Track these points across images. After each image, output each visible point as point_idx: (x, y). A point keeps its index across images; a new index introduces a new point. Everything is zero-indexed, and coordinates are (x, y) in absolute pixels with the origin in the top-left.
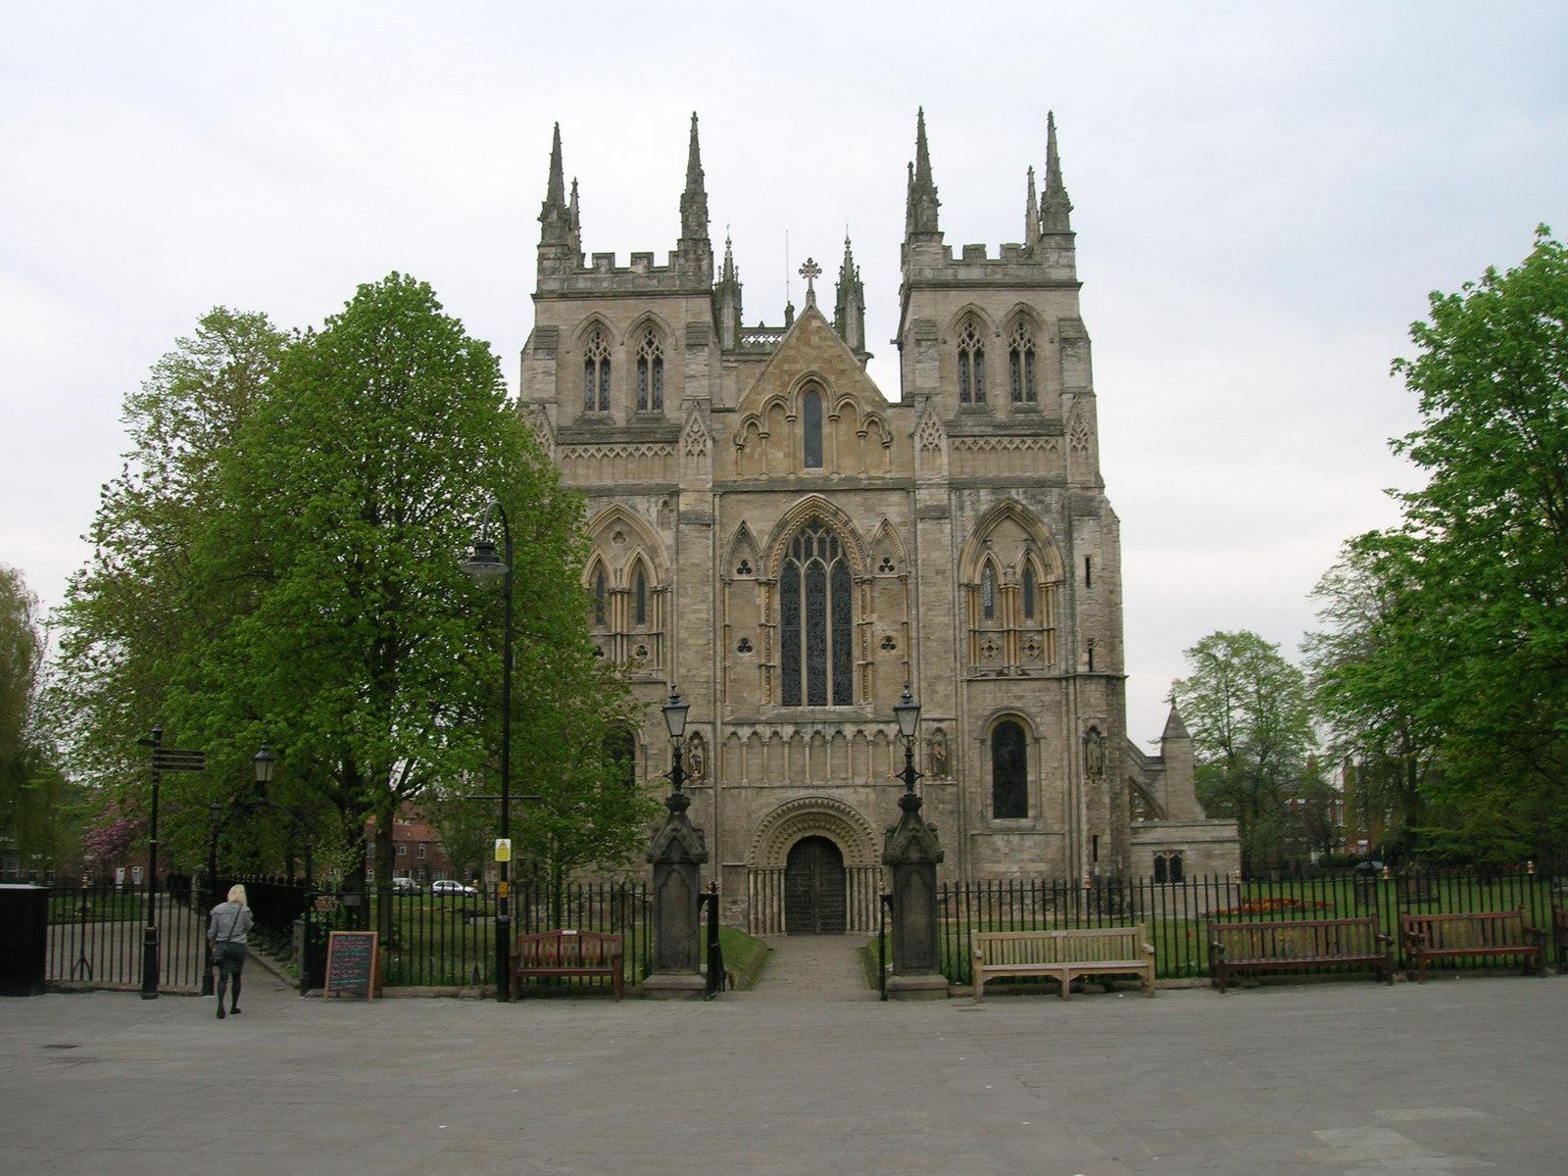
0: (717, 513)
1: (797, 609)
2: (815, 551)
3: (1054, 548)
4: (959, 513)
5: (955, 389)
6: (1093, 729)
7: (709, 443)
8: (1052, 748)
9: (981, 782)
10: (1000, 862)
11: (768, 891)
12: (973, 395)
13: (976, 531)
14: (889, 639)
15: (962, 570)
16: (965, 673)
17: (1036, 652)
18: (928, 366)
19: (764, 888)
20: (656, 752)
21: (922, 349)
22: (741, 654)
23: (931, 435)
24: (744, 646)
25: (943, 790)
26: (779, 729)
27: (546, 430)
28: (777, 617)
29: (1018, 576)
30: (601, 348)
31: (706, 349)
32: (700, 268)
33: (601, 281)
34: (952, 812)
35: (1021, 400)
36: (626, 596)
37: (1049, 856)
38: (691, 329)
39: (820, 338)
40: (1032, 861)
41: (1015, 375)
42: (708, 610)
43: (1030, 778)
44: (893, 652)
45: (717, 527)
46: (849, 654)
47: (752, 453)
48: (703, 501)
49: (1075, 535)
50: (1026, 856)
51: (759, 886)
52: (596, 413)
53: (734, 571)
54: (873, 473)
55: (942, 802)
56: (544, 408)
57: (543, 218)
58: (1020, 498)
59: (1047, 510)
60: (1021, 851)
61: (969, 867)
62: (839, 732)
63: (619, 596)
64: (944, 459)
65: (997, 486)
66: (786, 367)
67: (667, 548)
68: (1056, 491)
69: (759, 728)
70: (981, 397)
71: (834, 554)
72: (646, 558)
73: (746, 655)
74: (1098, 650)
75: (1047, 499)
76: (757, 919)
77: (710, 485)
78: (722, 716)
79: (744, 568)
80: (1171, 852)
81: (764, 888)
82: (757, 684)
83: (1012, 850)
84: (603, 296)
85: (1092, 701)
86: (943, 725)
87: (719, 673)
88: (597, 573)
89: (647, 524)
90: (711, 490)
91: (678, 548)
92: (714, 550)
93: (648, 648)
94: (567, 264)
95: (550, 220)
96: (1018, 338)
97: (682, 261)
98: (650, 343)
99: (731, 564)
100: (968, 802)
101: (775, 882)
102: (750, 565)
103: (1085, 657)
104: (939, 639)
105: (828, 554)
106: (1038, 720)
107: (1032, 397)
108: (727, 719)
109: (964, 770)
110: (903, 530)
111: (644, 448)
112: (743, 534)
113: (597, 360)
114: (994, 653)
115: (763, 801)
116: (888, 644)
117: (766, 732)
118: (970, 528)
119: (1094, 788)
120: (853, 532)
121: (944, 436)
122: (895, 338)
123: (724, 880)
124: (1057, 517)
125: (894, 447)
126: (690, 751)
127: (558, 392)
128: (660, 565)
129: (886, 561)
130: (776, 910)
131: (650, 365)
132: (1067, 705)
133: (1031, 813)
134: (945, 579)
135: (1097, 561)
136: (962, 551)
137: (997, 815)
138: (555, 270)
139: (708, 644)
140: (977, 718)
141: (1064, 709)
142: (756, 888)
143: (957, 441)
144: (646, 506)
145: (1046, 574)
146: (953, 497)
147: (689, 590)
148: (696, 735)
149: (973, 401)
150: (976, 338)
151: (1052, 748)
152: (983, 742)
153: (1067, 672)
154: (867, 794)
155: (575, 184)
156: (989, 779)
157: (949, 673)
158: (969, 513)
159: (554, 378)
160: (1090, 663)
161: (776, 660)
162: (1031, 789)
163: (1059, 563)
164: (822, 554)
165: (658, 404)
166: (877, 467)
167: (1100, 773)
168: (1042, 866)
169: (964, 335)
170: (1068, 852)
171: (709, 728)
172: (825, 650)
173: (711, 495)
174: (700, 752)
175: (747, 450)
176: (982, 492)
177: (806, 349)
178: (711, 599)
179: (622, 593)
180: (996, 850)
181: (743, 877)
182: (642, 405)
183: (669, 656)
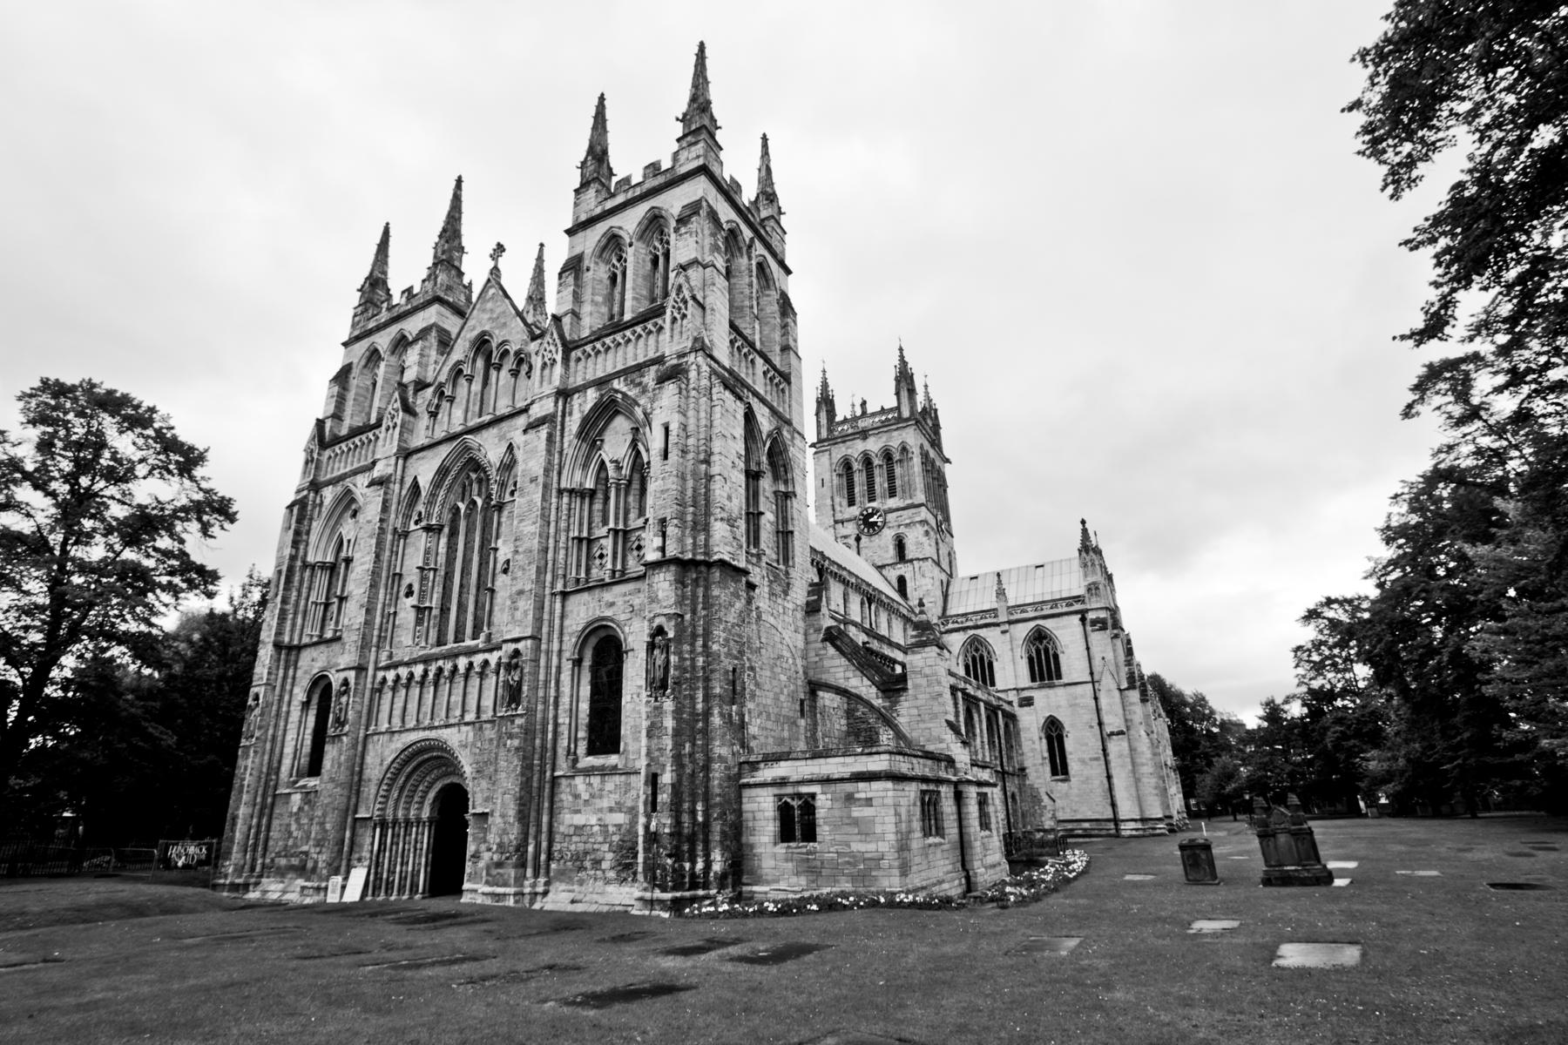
6: (660, 631)
9: (573, 712)
55: (511, 736)
74: (671, 530)
78: (376, 662)
85: (661, 595)
106: (626, 629)
119: (656, 708)
135: (674, 427)
137: (591, 751)
160: (663, 549)
167: (664, 686)
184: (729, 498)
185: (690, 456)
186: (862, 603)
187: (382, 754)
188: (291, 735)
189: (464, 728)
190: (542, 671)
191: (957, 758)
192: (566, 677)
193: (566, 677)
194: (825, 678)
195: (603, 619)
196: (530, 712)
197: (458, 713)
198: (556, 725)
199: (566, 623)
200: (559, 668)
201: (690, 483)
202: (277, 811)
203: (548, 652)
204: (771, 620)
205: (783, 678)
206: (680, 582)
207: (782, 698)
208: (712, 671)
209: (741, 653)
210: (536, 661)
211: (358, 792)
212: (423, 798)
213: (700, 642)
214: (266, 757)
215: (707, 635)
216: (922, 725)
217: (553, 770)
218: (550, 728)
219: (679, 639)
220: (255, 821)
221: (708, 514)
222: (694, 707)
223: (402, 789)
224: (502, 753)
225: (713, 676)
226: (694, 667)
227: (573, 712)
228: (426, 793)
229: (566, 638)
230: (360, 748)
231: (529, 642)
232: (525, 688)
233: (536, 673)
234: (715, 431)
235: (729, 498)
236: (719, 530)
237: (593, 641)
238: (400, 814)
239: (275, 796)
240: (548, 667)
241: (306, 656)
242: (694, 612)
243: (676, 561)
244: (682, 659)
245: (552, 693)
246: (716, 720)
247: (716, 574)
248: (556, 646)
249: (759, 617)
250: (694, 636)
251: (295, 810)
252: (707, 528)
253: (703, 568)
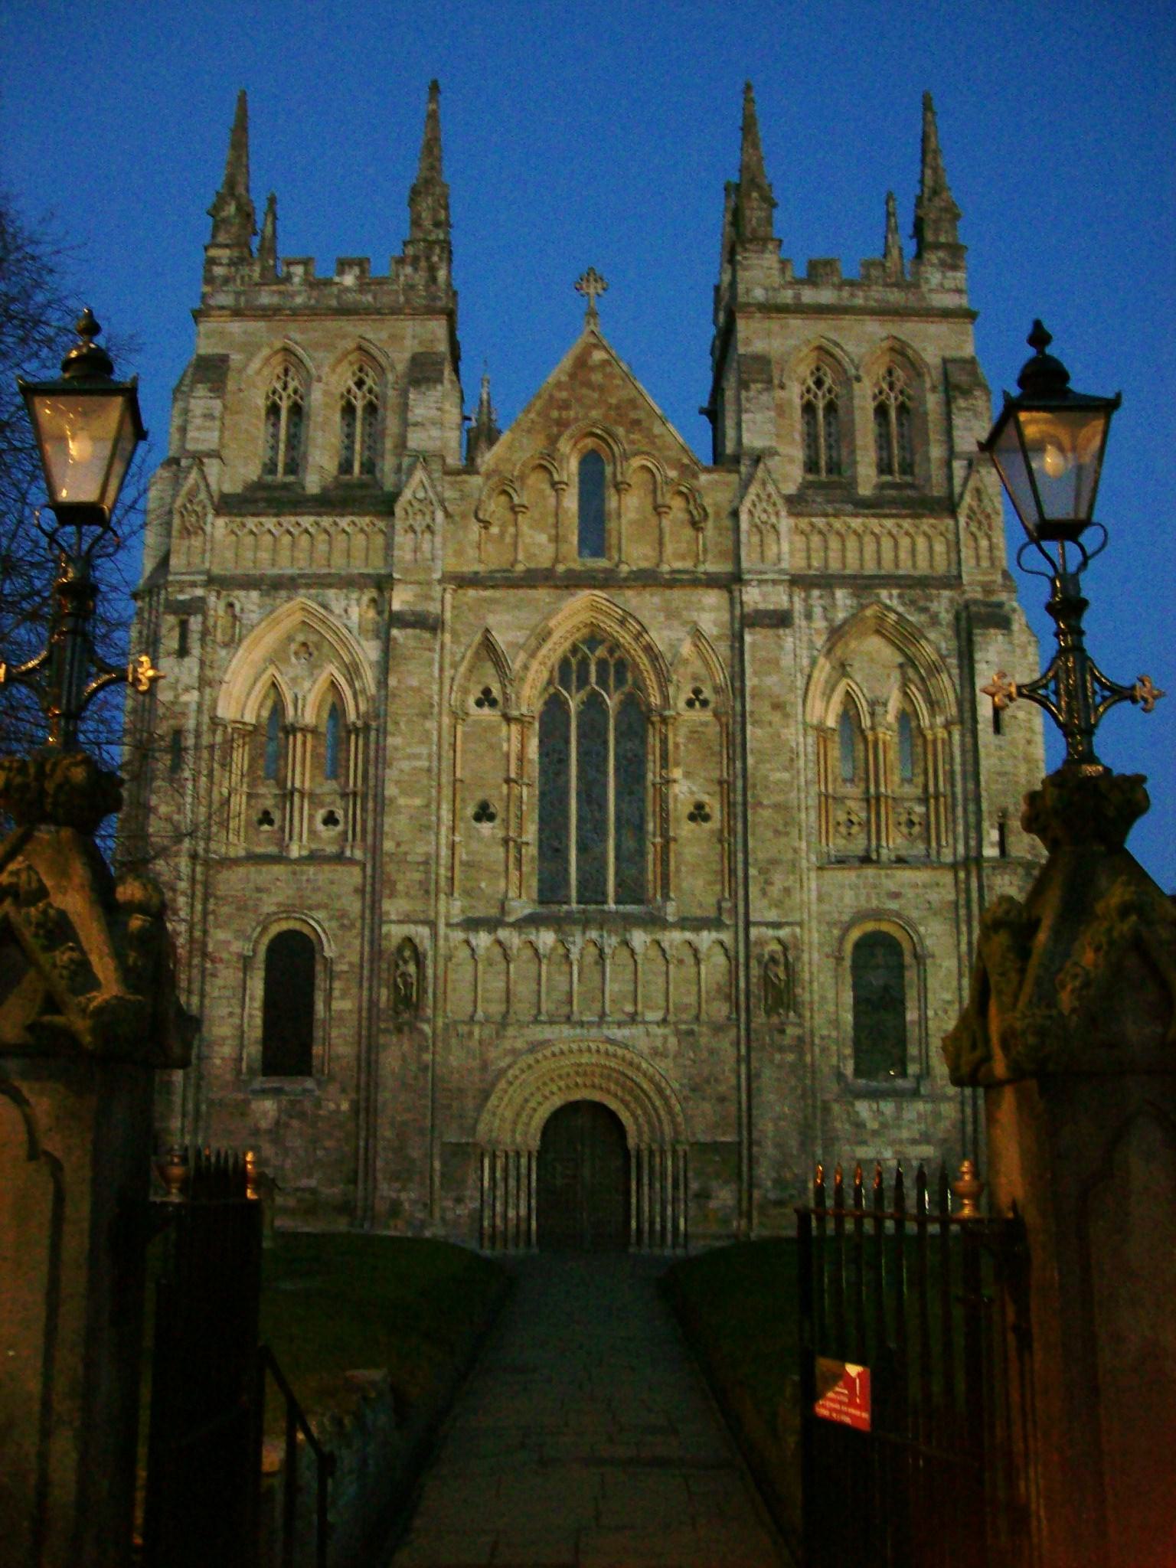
0: (448, 615)
1: (564, 761)
2: (593, 678)
3: (945, 676)
4: (804, 623)
5: (799, 454)
7: (440, 515)
8: (942, 973)
9: (836, 1023)
10: (864, 1143)
11: (512, 1183)
12: (823, 463)
13: (829, 651)
14: (699, 806)
15: (808, 709)
16: (813, 858)
17: (916, 829)
18: (759, 417)
19: (506, 1179)
20: (345, 968)
21: (752, 394)
22: (478, 825)
23: (765, 511)
24: (484, 813)
25: (782, 1032)
26: (533, 938)
27: (202, 496)
28: (533, 771)
29: (891, 718)
30: (290, 390)
31: (439, 387)
32: (433, 279)
33: (292, 296)
35: (891, 472)
36: (309, 736)
37: (941, 1135)
38: (416, 361)
39: (605, 376)
40: (914, 1142)
41: (883, 441)
42: (430, 756)
43: (911, 1015)
44: (707, 826)
45: (447, 637)
46: (640, 828)
47: (502, 534)
48: (428, 598)
49: (978, 656)
50: (905, 1134)
51: (498, 1175)
52: (280, 476)
53: (471, 701)
54: (678, 565)
55: (781, 1049)
56: (202, 463)
57: (214, 211)
58: (894, 603)
59: (935, 621)
61: (819, 1151)
62: (626, 943)
63: (299, 736)
64: (785, 547)
65: (863, 585)
66: (555, 414)
67: (371, 665)
68: (946, 593)
69: (503, 934)
70: (834, 467)
71: (620, 681)
72: (342, 681)
73: (486, 828)
75: (934, 607)
76: (494, 1226)
77: (437, 576)
78: (447, 917)
79: (486, 699)
81: (506, 1179)
82: (502, 868)
84: (295, 313)
86: (783, 933)
87: (444, 852)
88: (269, 703)
89: (345, 631)
90: (440, 582)
91: (384, 668)
92: (441, 670)
93: (340, 814)
94: (245, 270)
95: (224, 214)
96: (885, 386)
97: (409, 270)
98: (360, 384)
99: (465, 691)
100: (817, 1050)
101: (523, 1171)
102: (496, 692)
103: (994, 835)
104: (777, 807)
105: (611, 682)
106: (922, 929)
107: (907, 468)
108: (455, 920)
109: (811, 1003)
110: (723, 648)
111: (344, 522)
112: (488, 645)
113: (284, 405)
114: (855, 829)
115: (507, 1044)
116: (699, 814)
117: (512, 938)
118: (820, 641)
120: (648, 649)
121: (783, 513)
122: (705, 405)
123: (444, 1164)
124: (950, 633)
125: (710, 525)
126: (397, 966)
127: (222, 445)
128: (364, 691)
129: (697, 692)
130: (523, 1212)
131: (359, 413)
132: (968, 907)
133: (913, 1069)
134: (786, 716)
136: (810, 677)
138: (227, 280)
139: (427, 806)
140: (831, 924)
141: (962, 912)
142: (493, 1178)
143: (803, 523)
144: (344, 603)
145: (932, 714)
146: (796, 599)
147: (403, 726)
148: (408, 940)
149: (824, 474)
150: (826, 386)
151: (942, 973)
152: (839, 959)
153: (967, 858)
154: (665, 1038)
155: (272, 201)
156: (848, 1017)
157: (790, 855)
158: (820, 624)
159: (218, 423)
161: (531, 832)
162: (913, 1033)
163: (952, 697)
164: (602, 681)
165: (369, 467)
166: (683, 558)
168: (928, 1151)
169: (810, 382)
170: (969, 1128)
171: (424, 931)
172: (605, 821)
173: (438, 588)
174: (412, 968)
175: (495, 530)
176: (840, 594)
177: (585, 391)
178: (435, 738)
179: (304, 730)
180: (860, 1125)
181: (473, 1163)
182: (346, 467)
183: (370, 824)
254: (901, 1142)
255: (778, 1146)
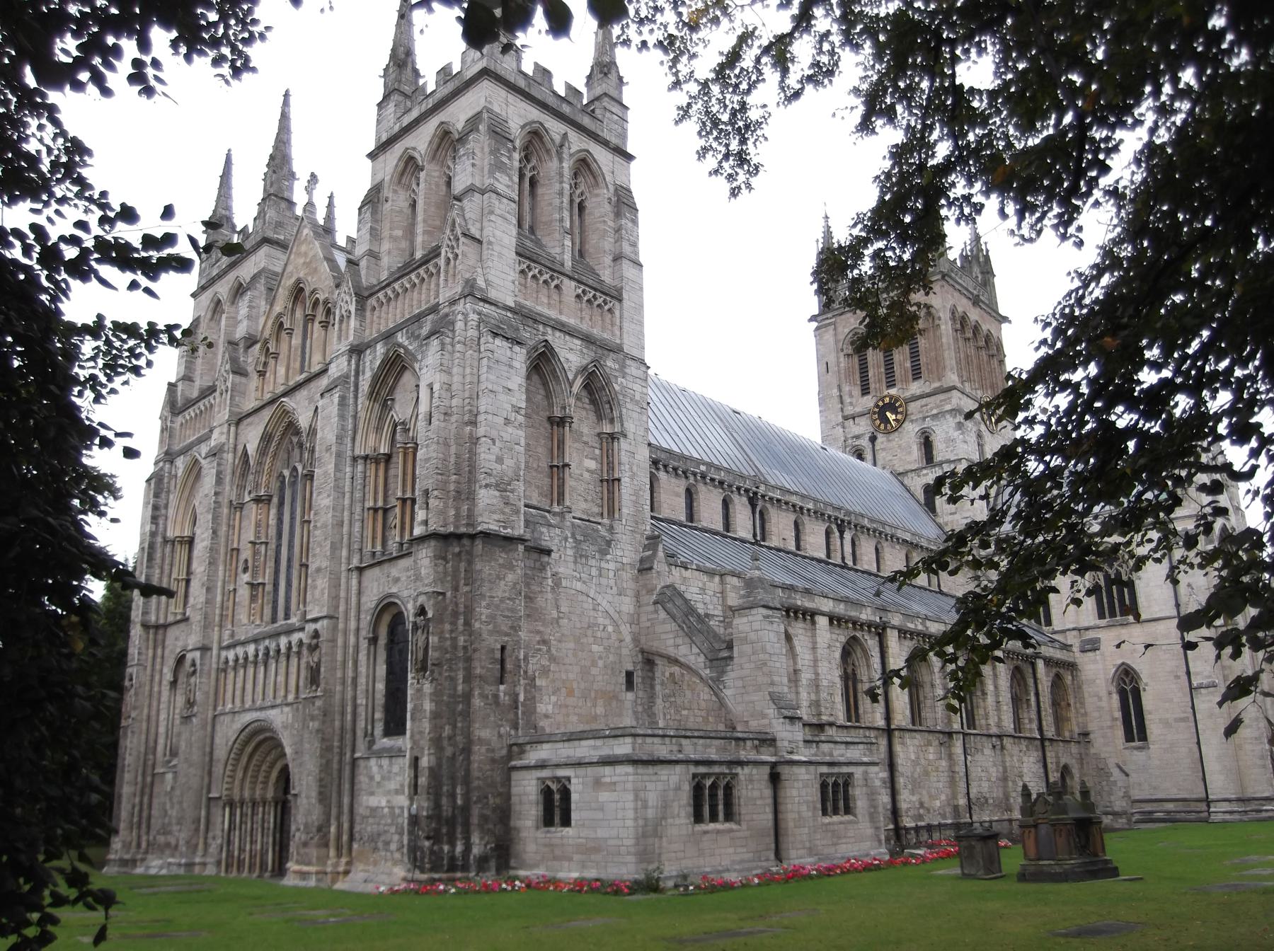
10: (372, 794)
25: (314, 704)
34: (318, 731)
50: (392, 785)
55: (313, 718)
60: (389, 779)
80: (558, 779)
83: (383, 778)
137: (388, 733)
180: (372, 778)
184: (500, 460)
185: (454, 419)
186: (828, 534)
187: (228, 731)
188: (163, 716)
189: (286, 709)
190: (340, 652)
191: (779, 736)
192: (362, 657)
193: (362, 657)
194: (656, 645)
195: (390, 595)
196: (328, 693)
197: (282, 693)
198: (355, 706)
199: (364, 599)
200: (357, 647)
201: (453, 449)
202: (156, 790)
203: (345, 632)
204: (579, 586)
205: (595, 648)
206: (440, 557)
207: (594, 671)
208: (475, 650)
209: (515, 628)
210: (333, 641)
211: (210, 773)
212: (267, 777)
213: (461, 621)
214: (143, 737)
215: (469, 611)
216: (746, 698)
217: (353, 751)
218: (349, 709)
219: (439, 619)
220: (137, 800)
221: (472, 480)
222: (455, 689)
223: (246, 769)
224: (306, 736)
225: (477, 655)
226: (455, 647)
227: (370, 693)
228: (269, 773)
229: (362, 616)
230: (209, 728)
231: (325, 622)
232: (322, 669)
233: (333, 654)
234: (483, 386)
235: (500, 460)
236: (486, 497)
237: (386, 619)
238: (247, 794)
239: (154, 775)
240: (345, 646)
241: (172, 633)
242: (456, 589)
243: (434, 536)
244: (442, 639)
245: (350, 673)
246: (477, 702)
247: (479, 545)
248: (353, 625)
249: (557, 584)
250: (455, 614)
251: (169, 789)
252: (472, 497)
253: (466, 542)
254: (389, 792)
255: (308, 797)
